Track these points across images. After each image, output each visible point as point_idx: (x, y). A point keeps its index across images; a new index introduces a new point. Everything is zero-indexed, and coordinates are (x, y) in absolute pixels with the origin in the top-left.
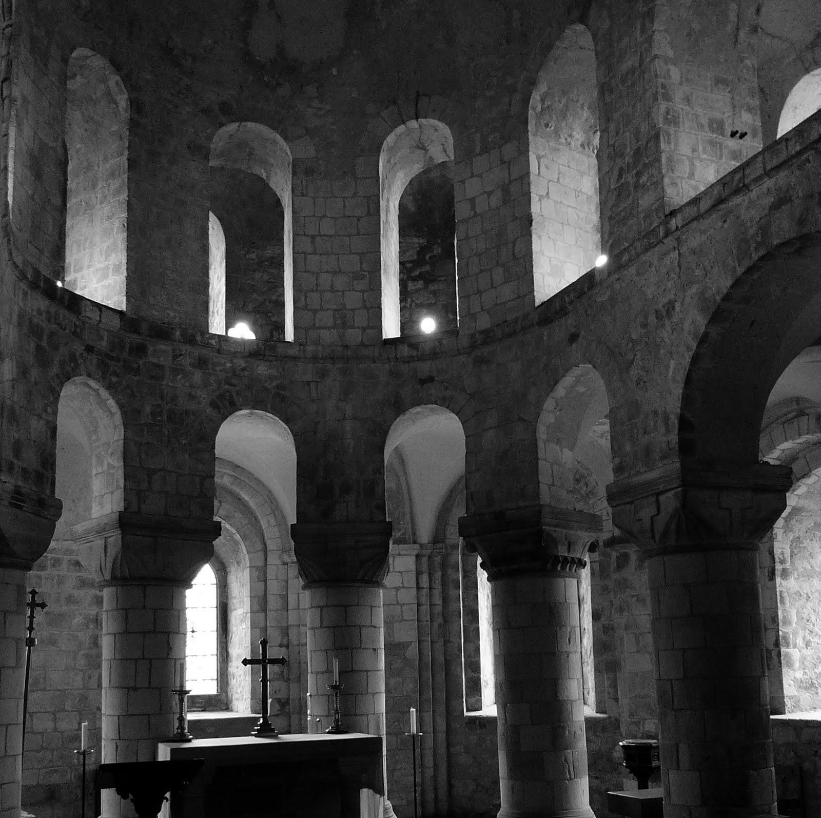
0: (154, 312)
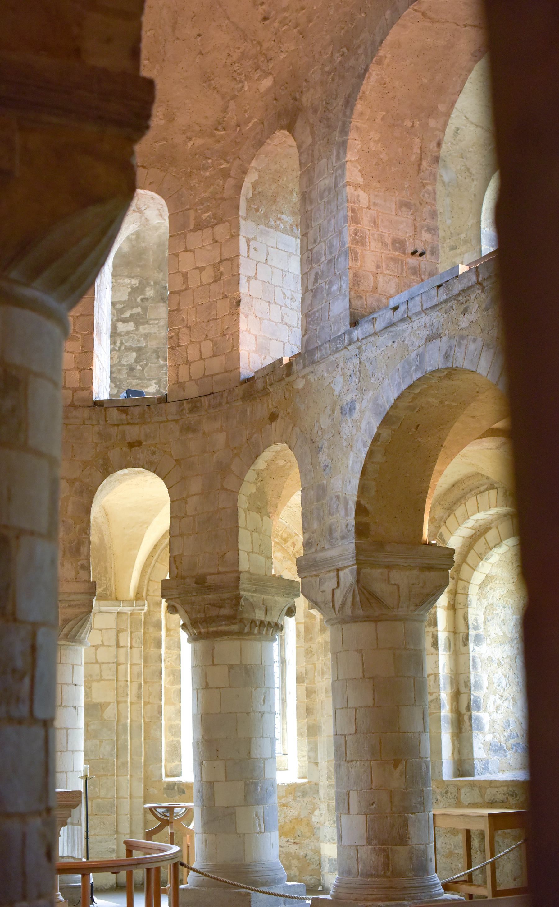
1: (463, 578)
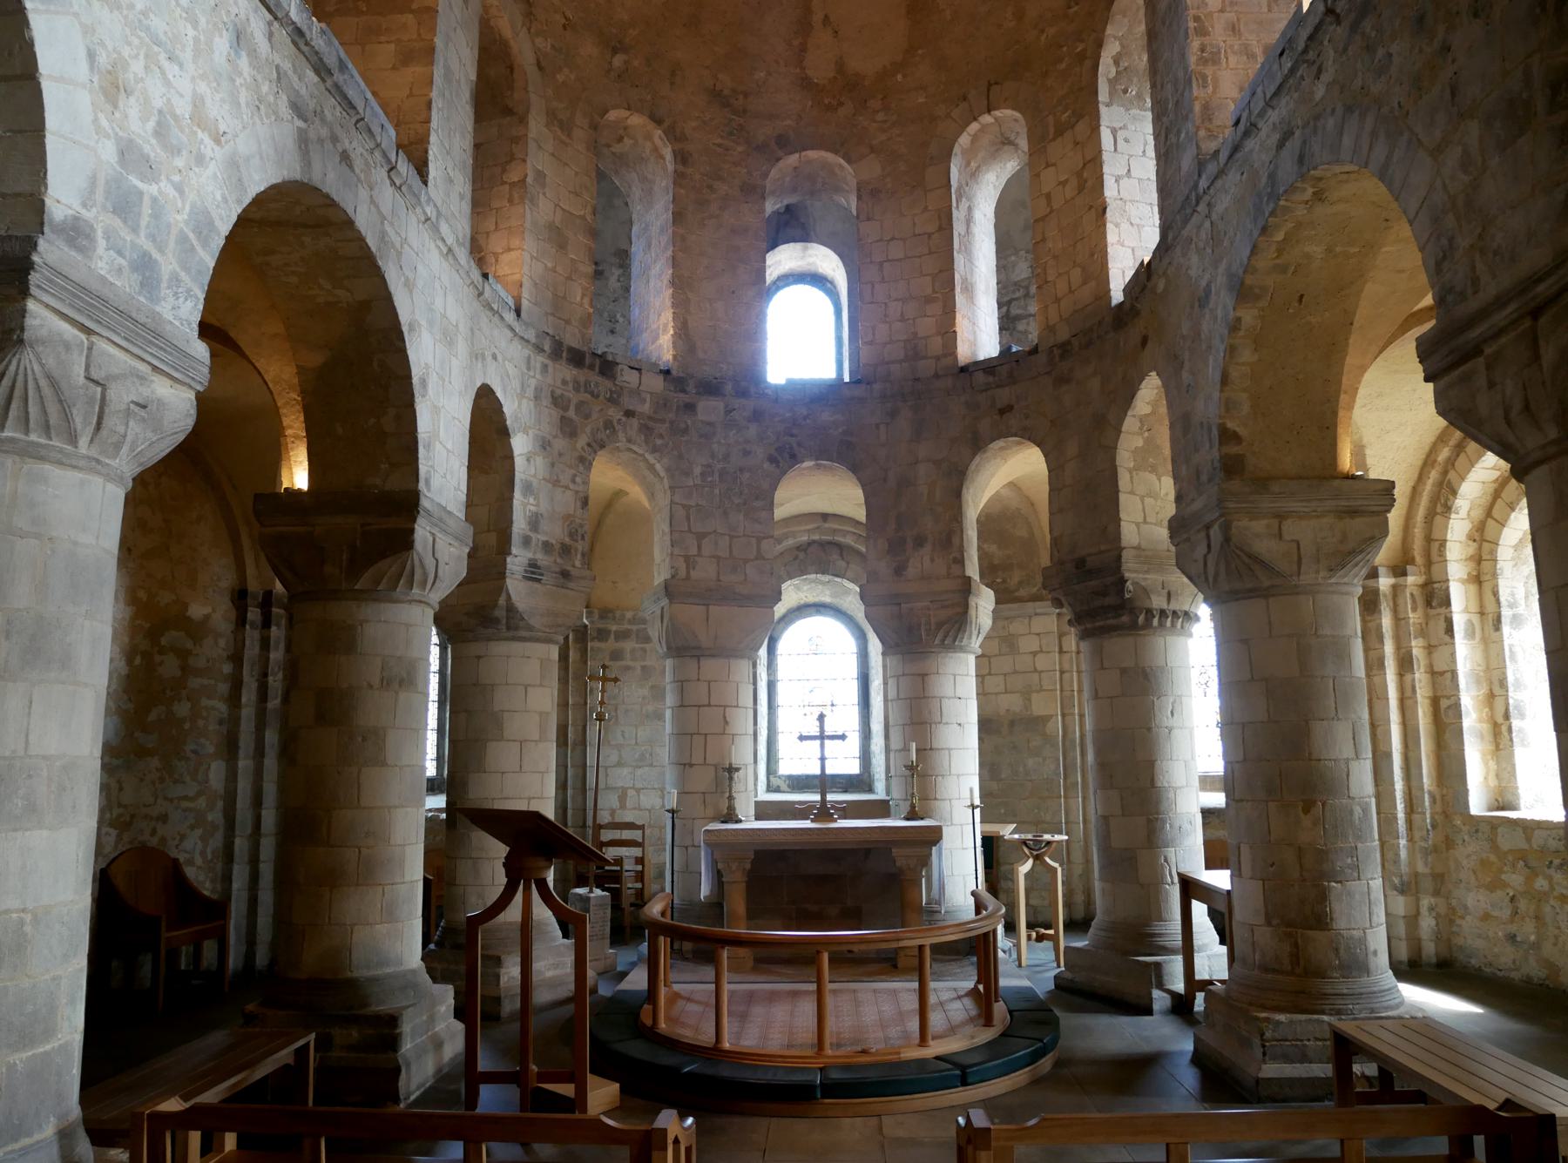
1: (1488, 539)
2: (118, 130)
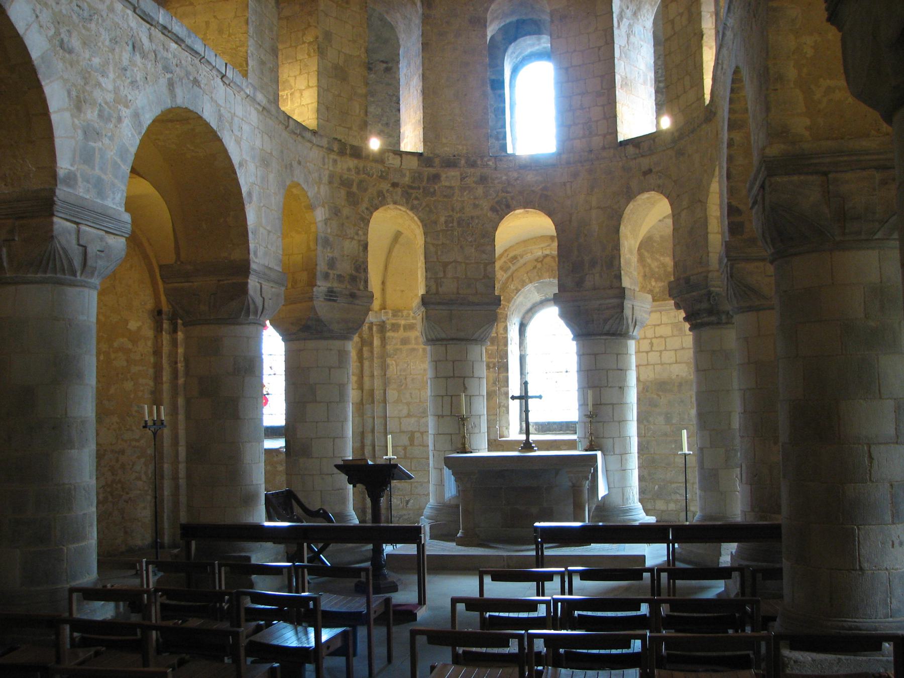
0: (446, 149)
2: (82, 122)
